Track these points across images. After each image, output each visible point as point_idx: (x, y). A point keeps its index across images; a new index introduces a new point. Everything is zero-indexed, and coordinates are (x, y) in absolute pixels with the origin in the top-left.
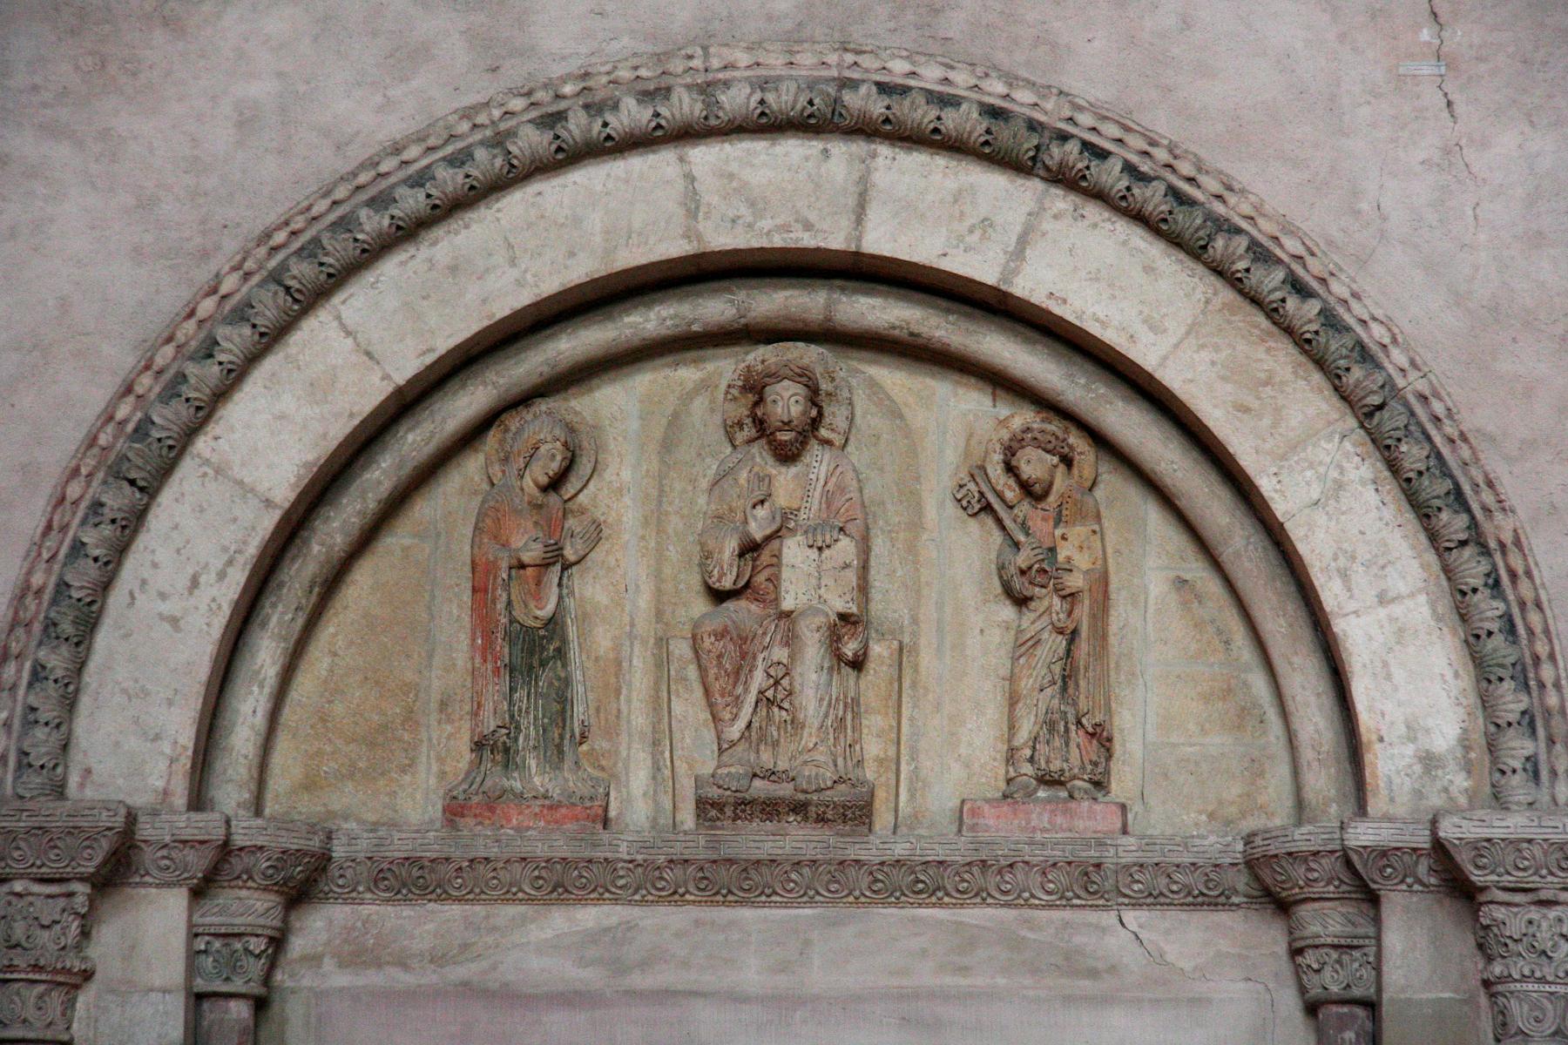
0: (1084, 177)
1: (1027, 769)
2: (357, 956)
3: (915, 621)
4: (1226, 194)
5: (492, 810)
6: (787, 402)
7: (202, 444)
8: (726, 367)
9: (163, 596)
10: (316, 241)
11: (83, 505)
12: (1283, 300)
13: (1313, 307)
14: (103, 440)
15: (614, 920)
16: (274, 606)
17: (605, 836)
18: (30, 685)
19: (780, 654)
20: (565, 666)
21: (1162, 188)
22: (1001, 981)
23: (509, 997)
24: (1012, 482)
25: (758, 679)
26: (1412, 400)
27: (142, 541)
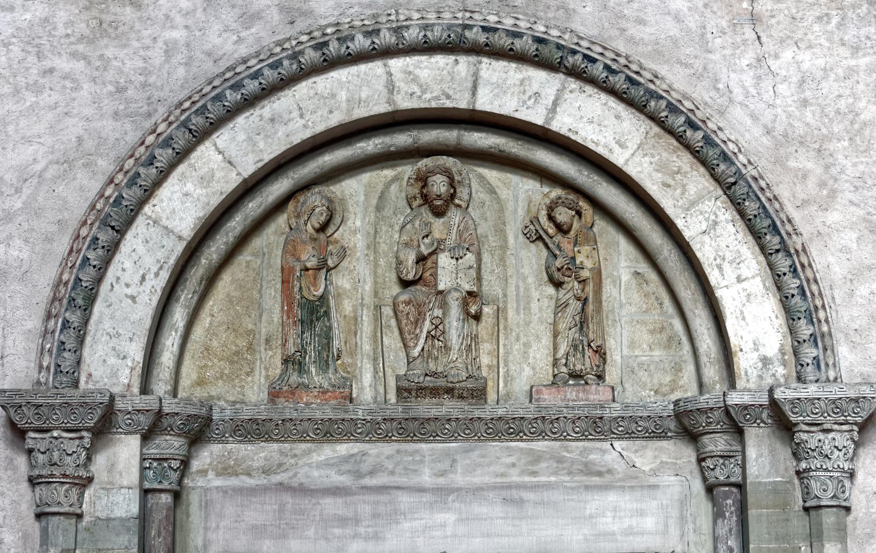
0: (585, 72)
1: (564, 369)
2: (225, 471)
3: (505, 295)
4: (655, 80)
5: (293, 394)
6: (439, 185)
7: (147, 209)
8: (407, 170)
9: (127, 285)
10: (204, 106)
11: (88, 239)
12: (685, 131)
13: (699, 135)
14: (98, 206)
15: (356, 450)
16: (182, 291)
17: (351, 407)
18: (61, 331)
19: (438, 312)
20: (329, 320)
21: (623, 77)
22: (553, 479)
23: (302, 490)
24: (551, 225)
25: (427, 325)
26: (750, 180)
27: (118, 257)
